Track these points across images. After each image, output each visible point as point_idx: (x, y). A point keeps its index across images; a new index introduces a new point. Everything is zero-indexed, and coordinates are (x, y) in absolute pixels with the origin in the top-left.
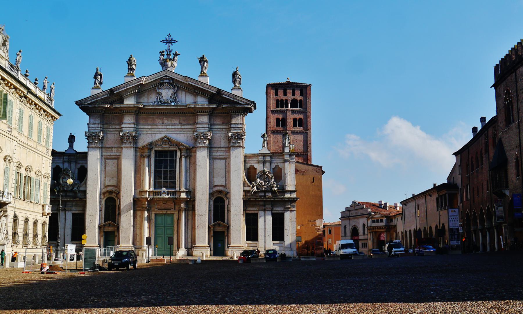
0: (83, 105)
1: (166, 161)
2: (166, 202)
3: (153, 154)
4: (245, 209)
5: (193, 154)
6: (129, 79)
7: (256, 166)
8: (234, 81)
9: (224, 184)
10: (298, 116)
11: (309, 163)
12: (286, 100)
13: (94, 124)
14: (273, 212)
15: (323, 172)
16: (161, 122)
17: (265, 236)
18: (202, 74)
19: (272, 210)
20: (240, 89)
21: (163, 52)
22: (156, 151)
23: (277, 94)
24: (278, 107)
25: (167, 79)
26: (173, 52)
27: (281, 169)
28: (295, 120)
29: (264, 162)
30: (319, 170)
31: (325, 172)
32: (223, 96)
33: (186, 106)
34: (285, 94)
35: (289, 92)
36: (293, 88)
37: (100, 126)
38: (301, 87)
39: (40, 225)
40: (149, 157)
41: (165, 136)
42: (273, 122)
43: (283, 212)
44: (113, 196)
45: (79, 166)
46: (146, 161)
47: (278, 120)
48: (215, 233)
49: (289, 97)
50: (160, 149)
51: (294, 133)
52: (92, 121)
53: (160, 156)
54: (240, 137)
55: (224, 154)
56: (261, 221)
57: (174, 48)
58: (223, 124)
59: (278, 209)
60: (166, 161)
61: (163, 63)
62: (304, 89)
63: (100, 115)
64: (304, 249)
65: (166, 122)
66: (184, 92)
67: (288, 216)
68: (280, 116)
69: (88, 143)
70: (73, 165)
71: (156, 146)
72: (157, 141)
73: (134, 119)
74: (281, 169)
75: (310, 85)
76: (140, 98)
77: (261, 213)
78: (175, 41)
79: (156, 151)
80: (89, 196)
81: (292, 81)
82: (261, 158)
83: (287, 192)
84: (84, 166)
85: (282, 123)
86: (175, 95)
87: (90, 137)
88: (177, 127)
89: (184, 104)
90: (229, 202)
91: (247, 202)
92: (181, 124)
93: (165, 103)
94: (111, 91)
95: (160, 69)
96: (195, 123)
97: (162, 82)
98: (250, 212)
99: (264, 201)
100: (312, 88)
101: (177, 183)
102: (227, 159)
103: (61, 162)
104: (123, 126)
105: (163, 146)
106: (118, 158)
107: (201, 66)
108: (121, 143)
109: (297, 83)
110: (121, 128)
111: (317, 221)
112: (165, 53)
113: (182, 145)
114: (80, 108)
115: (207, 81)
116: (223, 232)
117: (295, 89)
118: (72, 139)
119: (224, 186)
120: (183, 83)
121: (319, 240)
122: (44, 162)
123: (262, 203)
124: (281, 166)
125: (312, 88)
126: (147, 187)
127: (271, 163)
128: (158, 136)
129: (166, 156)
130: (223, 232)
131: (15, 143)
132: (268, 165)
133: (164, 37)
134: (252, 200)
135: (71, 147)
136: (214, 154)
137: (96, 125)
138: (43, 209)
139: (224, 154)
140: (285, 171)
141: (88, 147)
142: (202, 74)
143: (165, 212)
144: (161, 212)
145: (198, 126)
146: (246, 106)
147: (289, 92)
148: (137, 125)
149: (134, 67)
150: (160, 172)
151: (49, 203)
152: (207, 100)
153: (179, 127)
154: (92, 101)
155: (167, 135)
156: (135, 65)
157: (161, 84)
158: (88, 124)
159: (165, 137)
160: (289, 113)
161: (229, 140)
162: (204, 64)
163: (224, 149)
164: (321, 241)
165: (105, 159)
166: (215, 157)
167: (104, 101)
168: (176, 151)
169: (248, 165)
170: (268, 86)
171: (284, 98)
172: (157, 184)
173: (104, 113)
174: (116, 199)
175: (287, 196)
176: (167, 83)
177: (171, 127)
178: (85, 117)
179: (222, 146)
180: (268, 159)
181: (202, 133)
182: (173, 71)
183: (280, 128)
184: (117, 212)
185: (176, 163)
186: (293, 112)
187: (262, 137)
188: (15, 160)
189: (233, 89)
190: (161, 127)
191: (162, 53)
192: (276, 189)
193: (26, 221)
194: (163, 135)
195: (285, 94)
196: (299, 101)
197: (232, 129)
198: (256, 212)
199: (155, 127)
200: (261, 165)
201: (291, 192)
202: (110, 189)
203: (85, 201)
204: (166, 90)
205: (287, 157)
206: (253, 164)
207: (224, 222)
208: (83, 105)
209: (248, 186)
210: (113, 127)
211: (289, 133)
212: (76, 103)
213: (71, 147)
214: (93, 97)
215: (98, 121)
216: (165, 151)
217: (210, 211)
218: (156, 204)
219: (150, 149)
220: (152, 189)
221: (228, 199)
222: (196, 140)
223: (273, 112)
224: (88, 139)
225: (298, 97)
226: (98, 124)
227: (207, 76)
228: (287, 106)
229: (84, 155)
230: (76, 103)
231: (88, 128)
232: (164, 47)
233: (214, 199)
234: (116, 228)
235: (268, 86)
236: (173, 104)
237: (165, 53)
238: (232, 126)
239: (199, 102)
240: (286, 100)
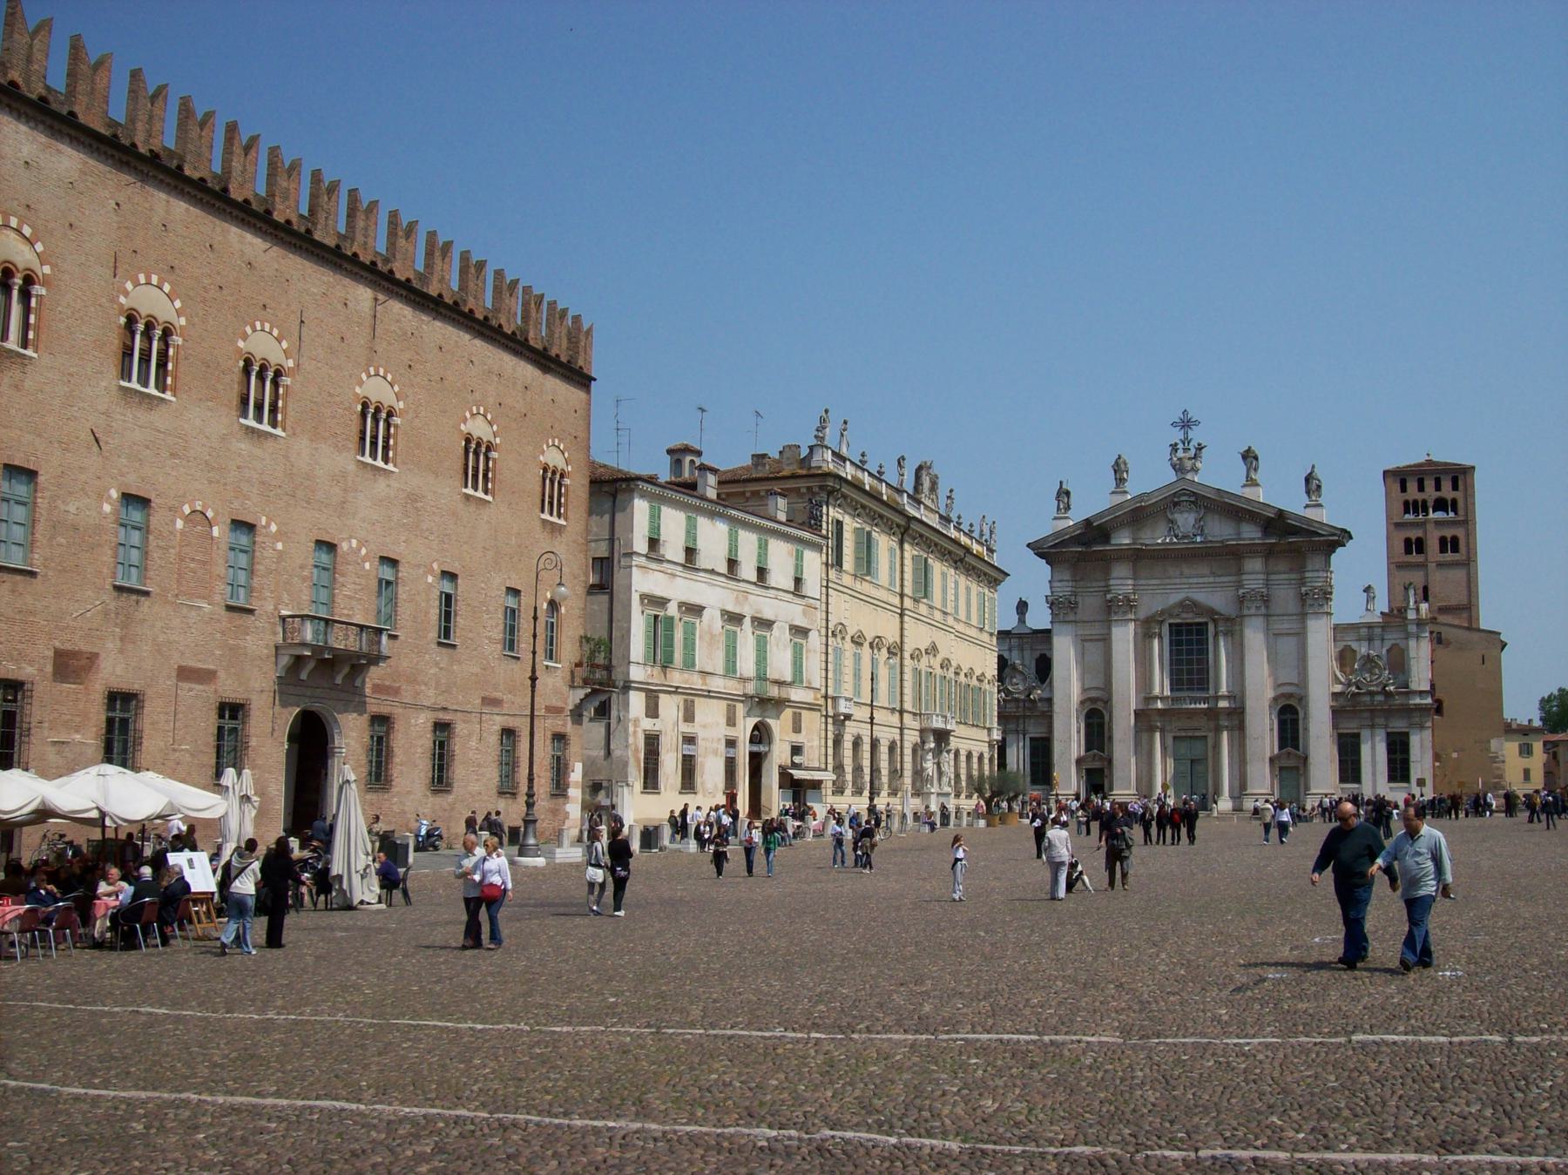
0: (1039, 549)
1: (1189, 642)
3: (1166, 629)
4: (1335, 726)
5: (1238, 628)
6: (1119, 499)
7: (1354, 645)
8: (1308, 492)
9: (1296, 682)
11: (1474, 626)
12: (1424, 502)
13: (1060, 581)
14: (1389, 730)
15: (1504, 645)
16: (1178, 573)
17: (1374, 774)
18: (1251, 482)
19: (1386, 727)
20: (1320, 505)
21: (1176, 444)
22: (1170, 625)
23: (1404, 489)
25: (1185, 495)
26: (1194, 444)
27: (1403, 651)
28: (1443, 541)
29: (1370, 639)
30: (1496, 642)
31: (1506, 644)
33: (1222, 542)
34: (1421, 488)
35: (1429, 484)
37: (1070, 584)
39: (986, 761)
42: (1400, 547)
43: (1406, 730)
44: (1099, 706)
45: (1037, 654)
46: (1156, 642)
47: (1408, 542)
48: (1281, 769)
49: (1430, 494)
50: (1178, 621)
51: (1440, 565)
52: (1058, 576)
53: (1179, 633)
54: (1326, 595)
55: (1294, 626)
56: (1365, 750)
57: (1196, 435)
58: (1291, 570)
60: (1189, 642)
61: (1178, 468)
62: (1459, 475)
65: (1186, 571)
66: (1216, 517)
67: (1415, 741)
68: (1414, 534)
69: (1052, 614)
70: (1027, 654)
71: (1171, 616)
74: (1403, 651)
75: (1473, 468)
76: (1139, 530)
77: (1365, 734)
78: (1197, 423)
79: (1170, 625)
80: (1056, 708)
81: (1434, 459)
82: (1364, 631)
83: (1415, 692)
84: (1045, 655)
85: (1415, 546)
86: (1202, 523)
87: (1053, 604)
88: (1205, 580)
89: (1219, 539)
90: (1305, 714)
91: (1337, 713)
92: (1213, 574)
93: (1184, 537)
94: (1088, 522)
95: (1171, 476)
96: (1240, 572)
97: (1176, 500)
98: (1345, 731)
99: (1372, 711)
100: (1476, 475)
101: (1211, 681)
102: (1301, 635)
103: (1006, 648)
104: (1112, 582)
105: (1184, 615)
106: (1106, 640)
107: (1245, 467)
108: (1109, 613)
109: (1446, 464)
110: (1108, 586)
111: (1492, 741)
112: (1180, 446)
113: (1217, 613)
115: (1260, 495)
116: (1297, 768)
117: (1442, 477)
118: (1022, 607)
119: (1297, 685)
120: (1215, 500)
122: (987, 657)
123: (1366, 715)
124: (1402, 645)
125: (1478, 476)
126: (1157, 691)
127: (1383, 640)
128: (1175, 598)
129: (1189, 632)
130: (1297, 768)
131: (953, 637)
132: (1377, 643)
133: (1177, 416)
135: (1022, 621)
136: (1276, 626)
137: (1066, 583)
138: (989, 735)
139: (1294, 626)
140: (1408, 654)
141: (1051, 622)
142: (1251, 482)
143: (1190, 734)
144: (1184, 734)
145: (1244, 577)
146: (1331, 538)
147: (1429, 484)
148: (1134, 579)
149: (1125, 475)
150: (1179, 662)
151: (996, 725)
152: (1259, 529)
153: (1211, 579)
155: (1190, 595)
156: (1127, 472)
157: (1176, 504)
158: (1050, 582)
159: (1187, 599)
160: (1430, 527)
161: (1303, 598)
162: (1252, 463)
163: (1295, 617)
165: (1083, 642)
166: (1276, 632)
167: (1076, 540)
168: (1206, 624)
169: (1341, 645)
170: (1385, 472)
171: (1420, 496)
172: (1176, 684)
174: (1105, 713)
177: (1195, 580)
178: (1042, 569)
179: (1290, 612)
180: (1378, 631)
181: (1253, 590)
182: (1196, 480)
183: (1415, 558)
184: (1106, 735)
185: (1207, 645)
187: (1364, 591)
188: (954, 664)
189: (1307, 506)
190: (1178, 581)
191: (1174, 448)
192: (1392, 688)
193: (969, 756)
195: (1421, 488)
196: (1449, 503)
197: (1308, 580)
198: (1355, 731)
199: (1168, 581)
200: (1365, 644)
201: (1421, 693)
202: (1093, 694)
203: (1051, 717)
204: (1186, 515)
205: (1412, 628)
206: (1349, 643)
207: (1296, 747)
208: (1039, 549)
209: (1341, 683)
210: (1094, 584)
211: (1432, 566)
212: (1028, 545)
213: (1022, 621)
214: (1057, 534)
215: (1067, 577)
216: (1187, 624)
217: (1272, 730)
219: (1162, 622)
220: (1167, 692)
221: (1306, 708)
222: (1242, 602)
223: (1398, 525)
224: (1050, 608)
225: (1447, 492)
226: (1068, 581)
227: (1257, 485)
228: (1425, 510)
229: (1047, 633)
230: (1028, 545)
231: (1051, 588)
232: (1177, 435)
233: (1278, 708)
234: (1106, 763)
235: (1385, 472)
236: (1199, 539)
237: (1180, 446)
238: (1307, 575)
239: (1245, 535)
240: (1424, 502)
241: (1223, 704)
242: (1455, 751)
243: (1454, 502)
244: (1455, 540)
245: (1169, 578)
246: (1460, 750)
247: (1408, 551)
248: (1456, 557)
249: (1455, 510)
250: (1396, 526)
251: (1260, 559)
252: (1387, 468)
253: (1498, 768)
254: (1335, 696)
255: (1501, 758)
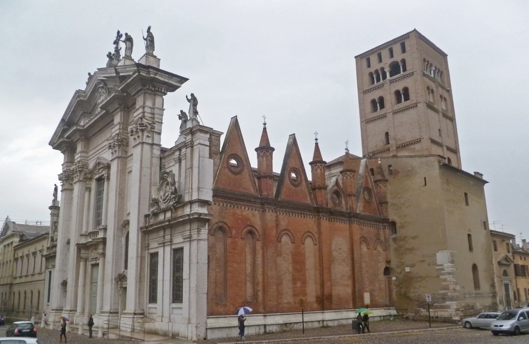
2: (95, 248)
3: (93, 185)
10: (400, 86)
23: (369, 66)
24: (373, 83)
28: (397, 93)
32: (121, 74)
34: (380, 60)
35: (385, 54)
36: (390, 47)
38: (400, 40)
40: (89, 189)
41: (98, 158)
47: (374, 102)
51: (395, 113)
59: (178, 240)
63: (68, 152)
64: (419, 307)
68: (375, 95)
72: (95, 167)
73: (82, 145)
105: (100, 171)
114: (54, 148)
121: (444, 291)
134: (150, 229)
147: (385, 54)
154: (57, 139)
164: (447, 293)
173: (70, 150)
175: (187, 210)
176: (99, 88)
183: (379, 112)
186: (391, 82)
194: (97, 156)
195: (380, 60)
196: (401, 64)
199: (97, 149)
201: (191, 203)
218: (91, 251)
219: (91, 179)
225: (398, 57)
228: (384, 77)
240: (382, 69)
241: (101, 235)
242: (407, 266)
243: (404, 61)
244: (406, 90)
245: (97, 147)
246: (412, 266)
247: (375, 109)
248: (408, 103)
249: (405, 70)
250: (362, 92)
251: (119, 114)
252: (357, 55)
253: (445, 280)
254: (147, 216)
255: (447, 270)
